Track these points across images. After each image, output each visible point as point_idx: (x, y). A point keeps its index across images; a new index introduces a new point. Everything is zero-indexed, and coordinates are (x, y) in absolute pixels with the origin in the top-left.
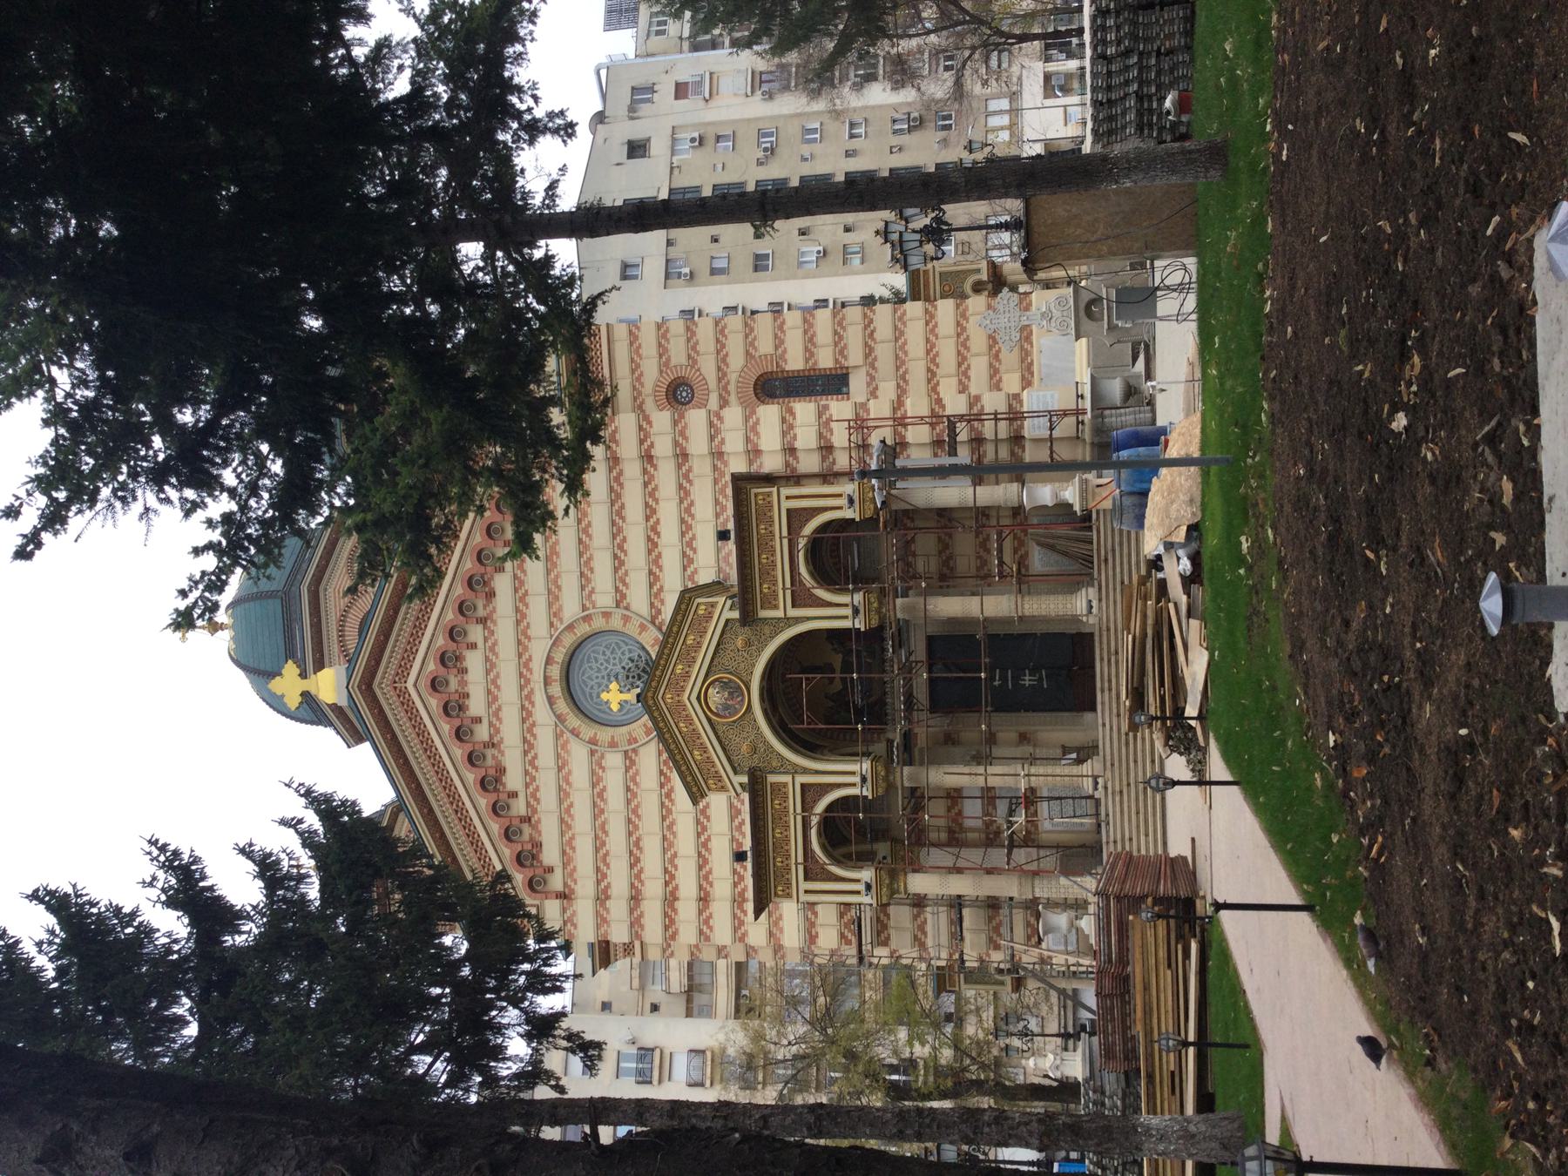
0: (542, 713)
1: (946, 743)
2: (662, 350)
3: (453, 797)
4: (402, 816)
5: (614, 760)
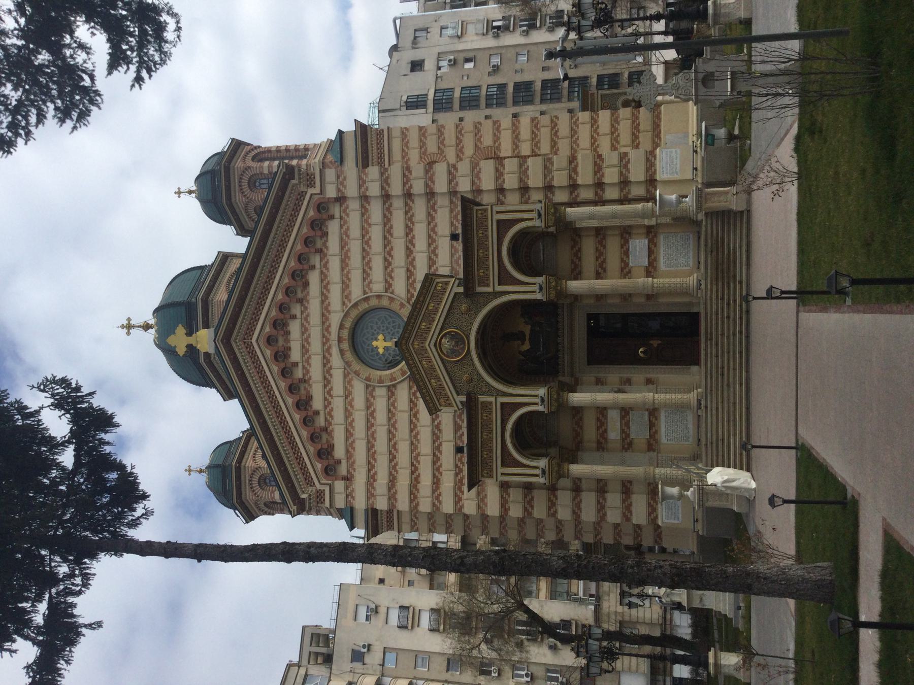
0: (336, 360)
1: (597, 384)
2: (422, 144)
3: (279, 414)
4: (253, 438)
5: (381, 392)
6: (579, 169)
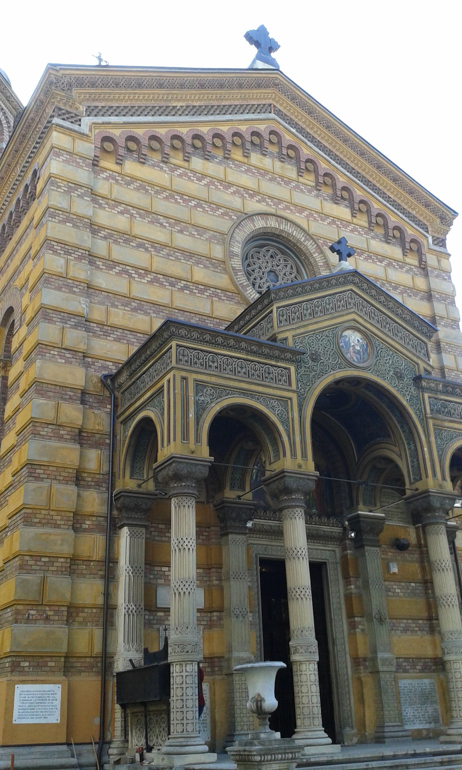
0: (253, 206)
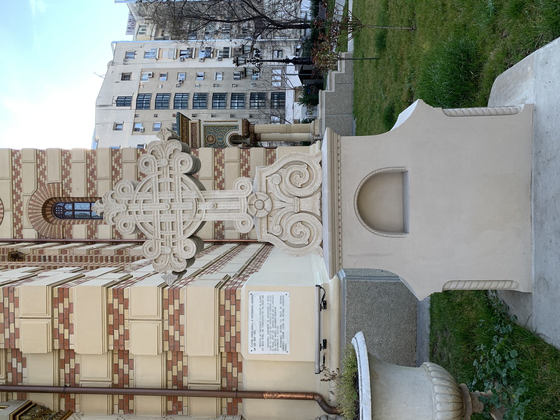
6: (74, 318)
